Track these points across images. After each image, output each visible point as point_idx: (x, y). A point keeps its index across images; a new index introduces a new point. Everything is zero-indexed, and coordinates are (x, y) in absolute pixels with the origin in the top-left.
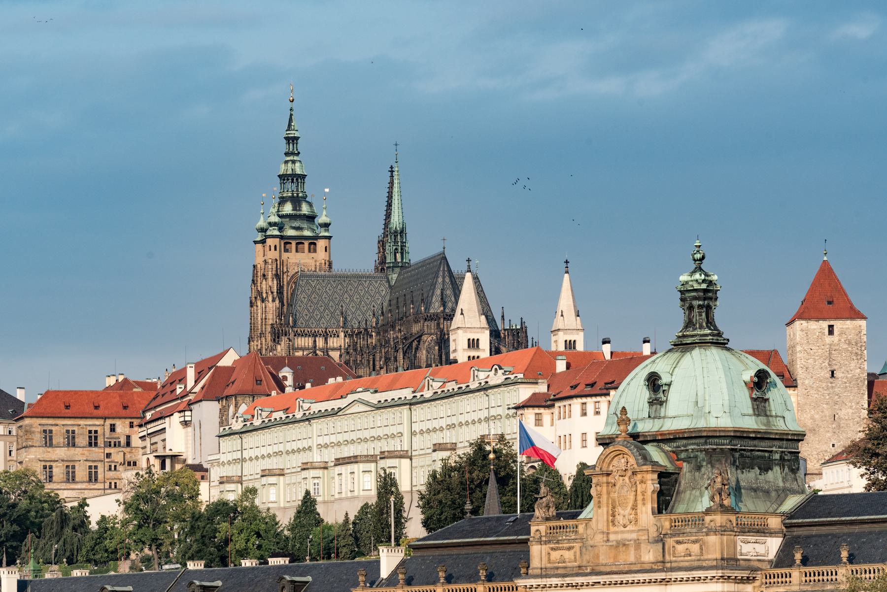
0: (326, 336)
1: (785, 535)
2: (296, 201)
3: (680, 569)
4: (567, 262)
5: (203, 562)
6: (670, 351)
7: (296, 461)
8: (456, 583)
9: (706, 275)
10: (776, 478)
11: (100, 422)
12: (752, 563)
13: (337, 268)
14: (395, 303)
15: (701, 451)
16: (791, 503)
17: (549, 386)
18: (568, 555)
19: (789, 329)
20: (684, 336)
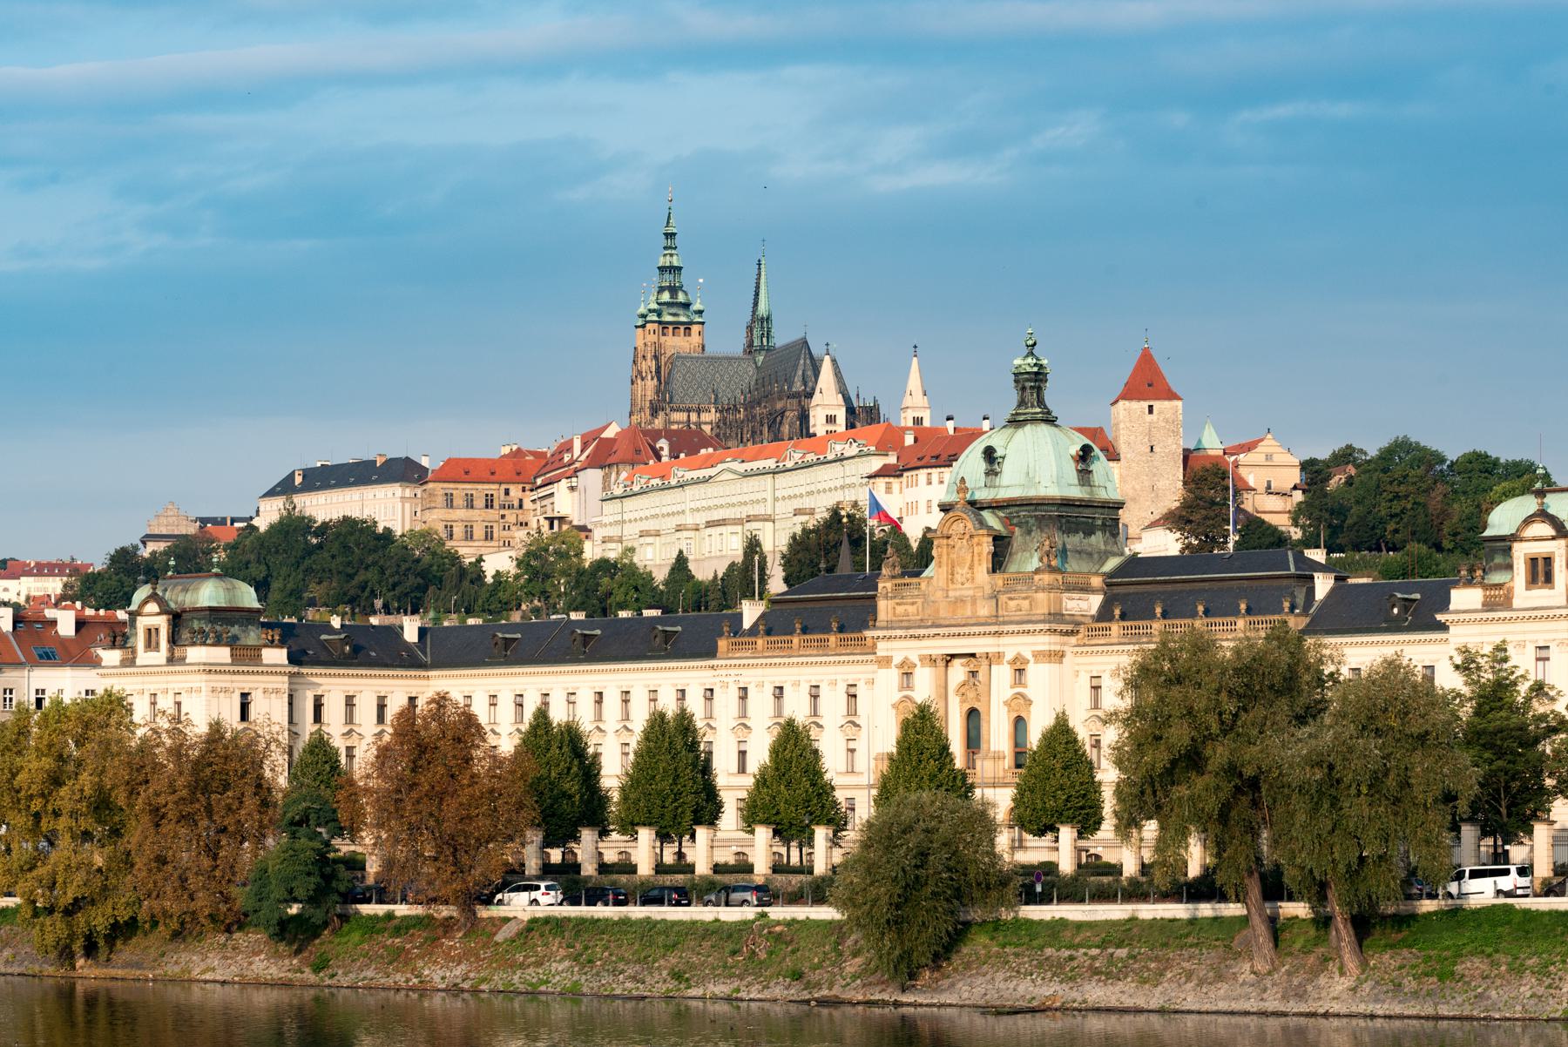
0: (699, 412)
1: (1105, 594)
2: (673, 290)
3: (1011, 623)
4: (915, 347)
5: (584, 613)
6: (1004, 427)
7: (671, 523)
8: (810, 633)
9: (1037, 359)
10: (1098, 542)
11: (495, 486)
12: (1076, 618)
13: (709, 351)
14: (761, 383)
15: (1031, 517)
16: (1112, 564)
17: (898, 458)
18: (911, 609)
19: (1114, 409)
20: (1017, 414)
